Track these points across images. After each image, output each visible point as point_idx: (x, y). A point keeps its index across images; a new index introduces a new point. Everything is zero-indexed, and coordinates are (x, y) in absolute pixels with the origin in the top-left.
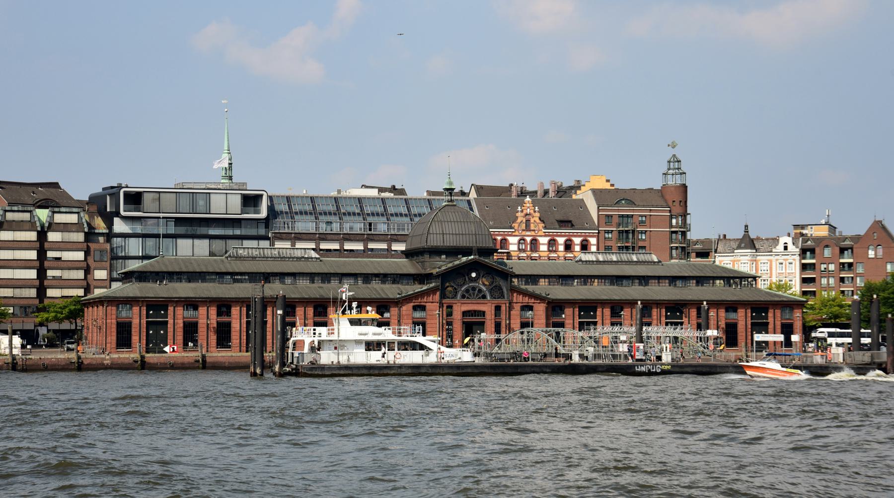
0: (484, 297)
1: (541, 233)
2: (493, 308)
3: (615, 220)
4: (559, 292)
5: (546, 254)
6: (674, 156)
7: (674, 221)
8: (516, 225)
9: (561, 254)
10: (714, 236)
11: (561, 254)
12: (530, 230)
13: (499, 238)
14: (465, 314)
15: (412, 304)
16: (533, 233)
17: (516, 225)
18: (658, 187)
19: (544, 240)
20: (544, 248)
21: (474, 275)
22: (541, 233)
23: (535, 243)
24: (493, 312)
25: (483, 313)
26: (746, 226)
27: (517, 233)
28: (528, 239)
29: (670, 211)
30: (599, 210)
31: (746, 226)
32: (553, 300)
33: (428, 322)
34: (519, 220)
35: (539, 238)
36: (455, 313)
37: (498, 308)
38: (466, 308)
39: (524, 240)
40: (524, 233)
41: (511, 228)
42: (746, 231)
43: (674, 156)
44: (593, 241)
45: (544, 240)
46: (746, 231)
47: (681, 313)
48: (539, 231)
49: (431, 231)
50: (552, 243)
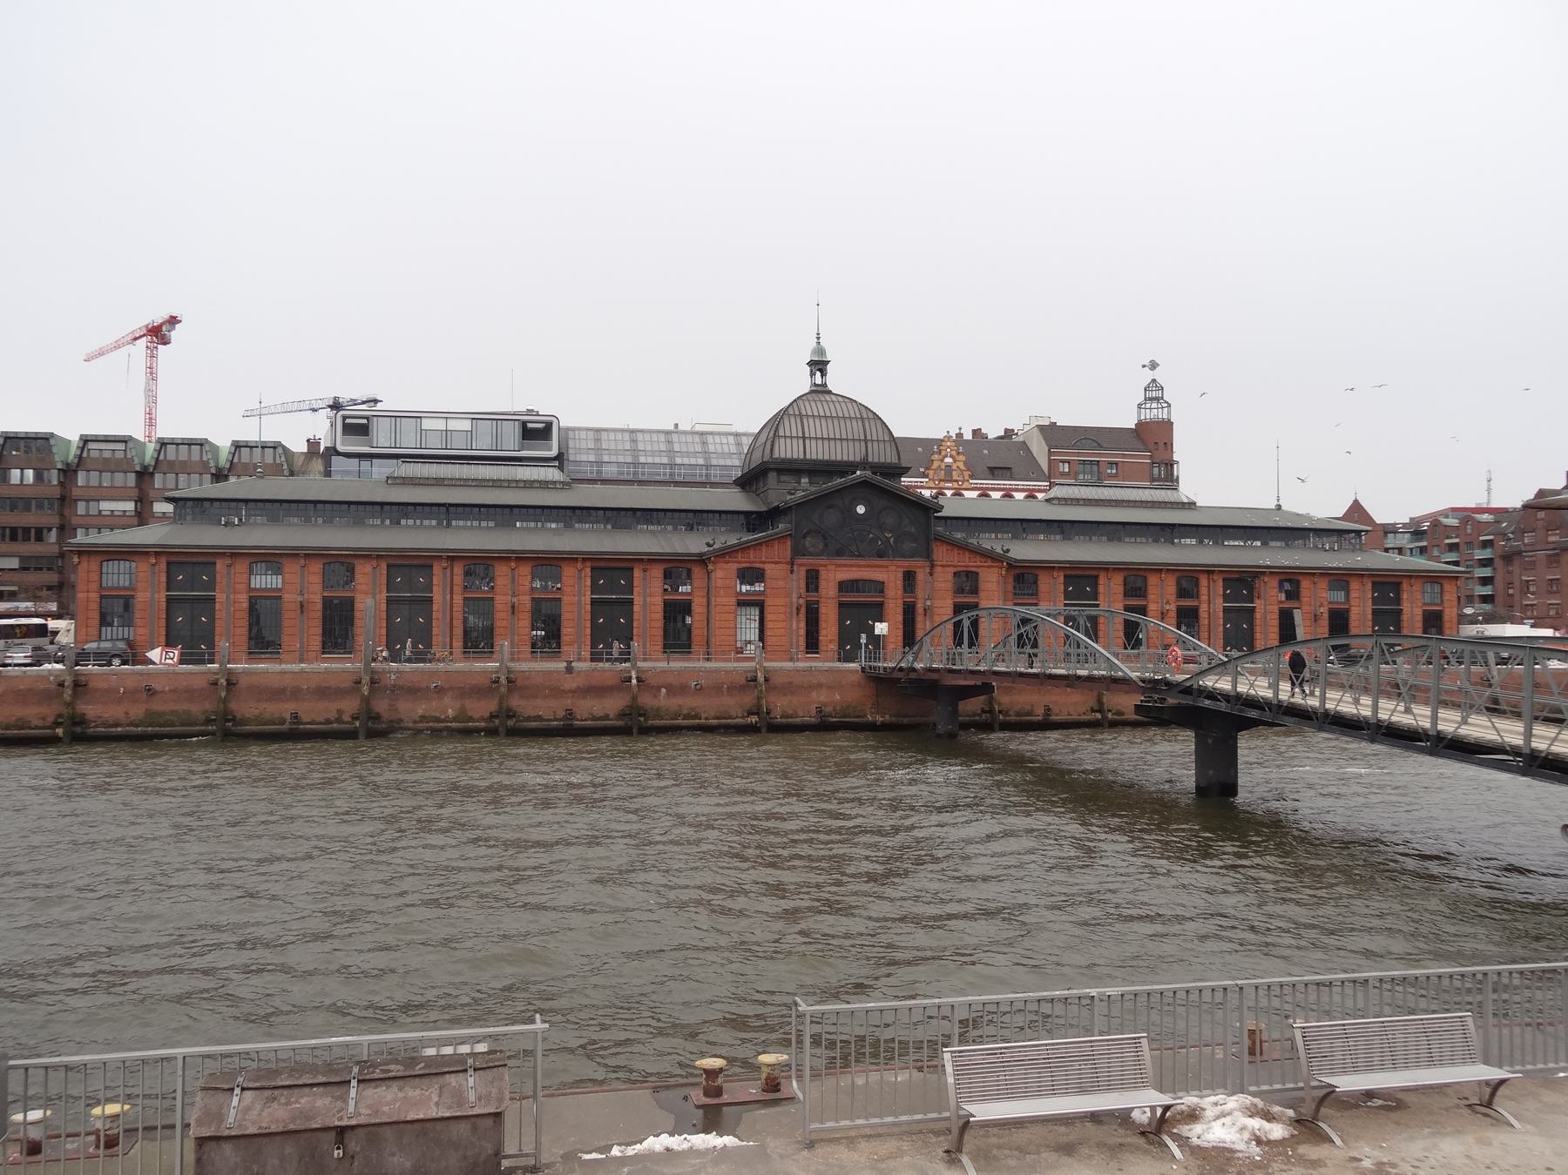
2: (900, 576)
4: (1025, 550)
6: (1154, 381)
7: (1156, 470)
8: (931, 473)
12: (951, 481)
14: (844, 586)
15: (736, 566)
17: (931, 473)
18: (1131, 423)
24: (900, 583)
25: (880, 587)
30: (1050, 454)
33: (768, 602)
34: (935, 465)
36: (823, 584)
37: (909, 578)
43: (1154, 381)
47: (1251, 590)
49: (781, 433)
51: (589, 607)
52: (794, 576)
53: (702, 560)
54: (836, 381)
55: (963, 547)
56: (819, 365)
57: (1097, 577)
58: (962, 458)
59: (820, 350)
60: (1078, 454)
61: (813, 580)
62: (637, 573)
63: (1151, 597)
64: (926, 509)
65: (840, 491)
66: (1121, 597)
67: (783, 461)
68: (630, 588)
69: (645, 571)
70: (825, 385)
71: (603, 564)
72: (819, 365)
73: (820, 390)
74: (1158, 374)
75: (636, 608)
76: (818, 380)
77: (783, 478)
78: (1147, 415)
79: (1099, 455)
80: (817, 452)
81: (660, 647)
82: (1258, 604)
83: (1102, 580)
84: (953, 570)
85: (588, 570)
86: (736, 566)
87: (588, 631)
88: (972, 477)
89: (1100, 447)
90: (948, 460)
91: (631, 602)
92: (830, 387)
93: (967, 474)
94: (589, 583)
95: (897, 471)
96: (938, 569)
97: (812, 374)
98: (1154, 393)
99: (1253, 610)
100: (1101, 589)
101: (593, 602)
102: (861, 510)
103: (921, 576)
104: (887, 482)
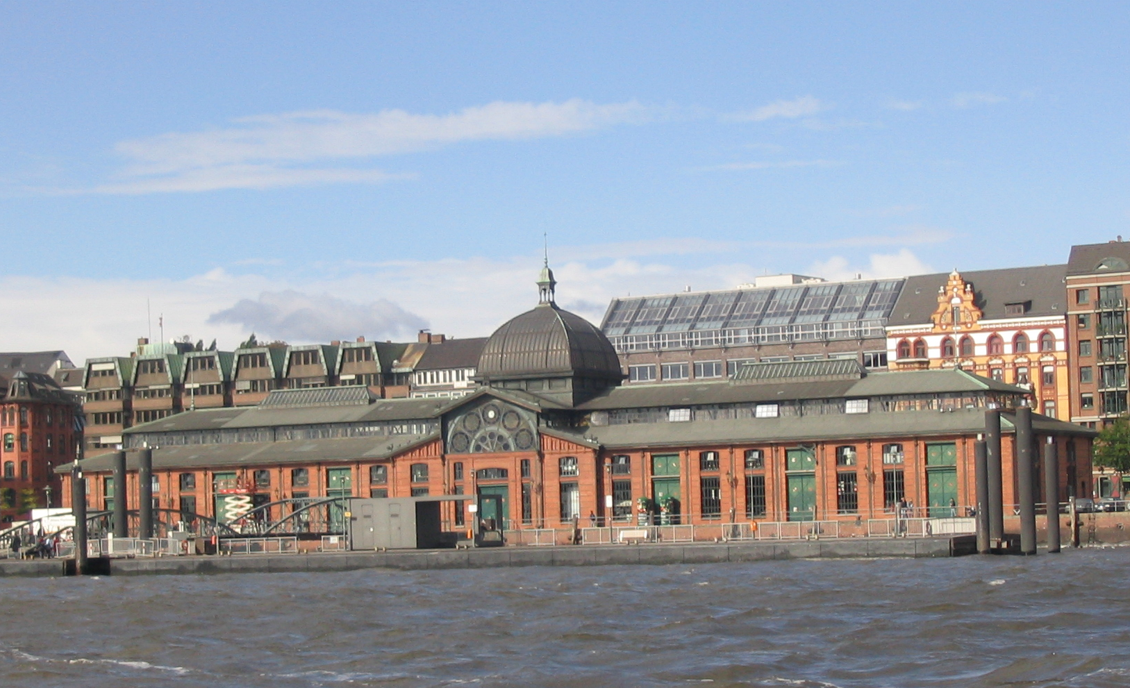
0: (506, 447)
2: (519, 464)
3: (1091, 297)
5: (984, 361)
8: (937, 317)
9: (1034, 358)
10: (134, 347)
11: (1034, 358)
13: (912, 340)
14: (478, 474)
16: (963, 328)
17: (937, 317)
19: (980, 339)
20: (980, 350)
23: (967, 345)
25: (503, 473)
27: (938, 329)
34: (941, 309)
35: (972, 335)
38: (480, 465)
41: (929, 322)
44: (1059, 333)
45: (980, 339)
50: (994, 343)
60: (1097, 280)
61: (458, 468)
88: (983, 317)
90: (956, 301)
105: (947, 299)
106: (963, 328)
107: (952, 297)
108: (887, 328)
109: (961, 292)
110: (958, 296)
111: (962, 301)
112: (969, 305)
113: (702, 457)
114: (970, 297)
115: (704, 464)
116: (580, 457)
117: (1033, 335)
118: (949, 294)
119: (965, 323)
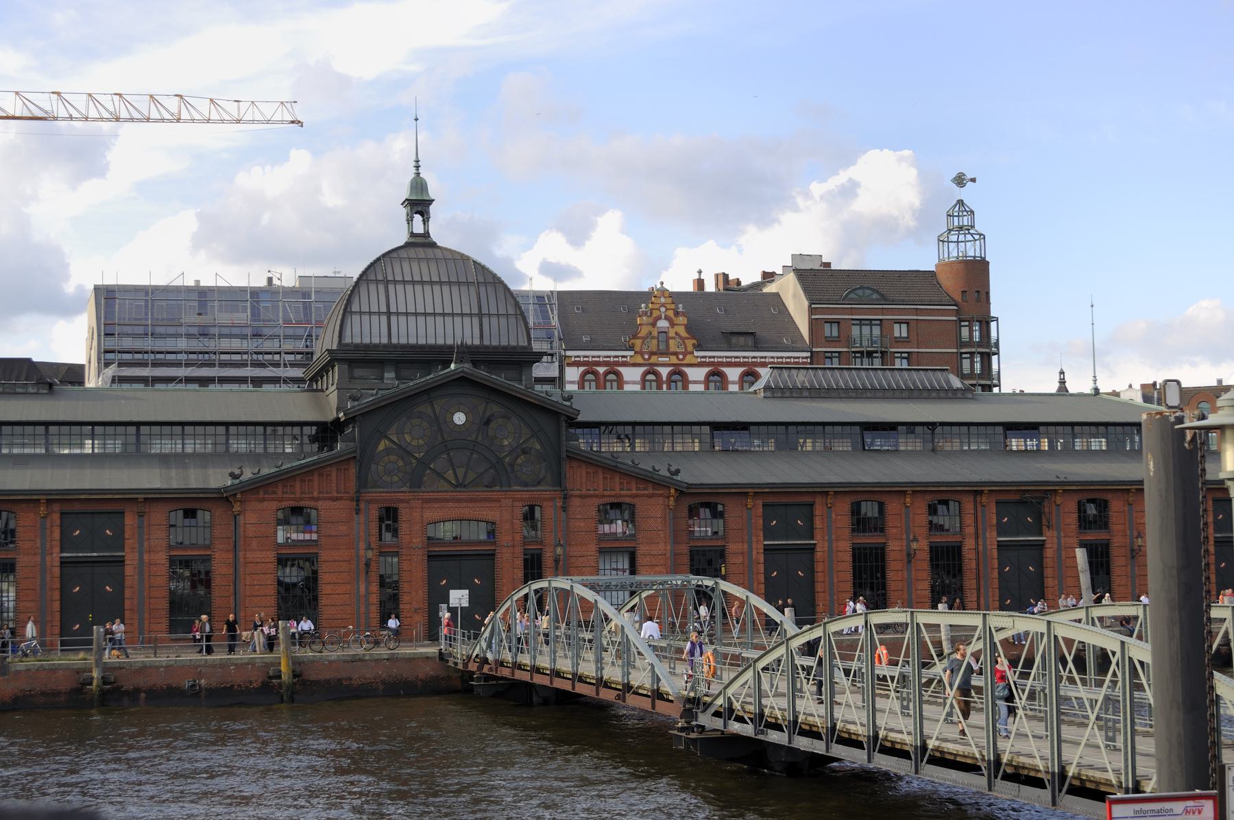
1: (689, 359)
7: (965, 332)
8: (638, 342)
12: (666, 353)
16: (674, 360)
17: (638, 342)
19: (697, 374)
21: (459, 418)
22: (689, 359)
26: (1062, 373)
27: (639, 360)
28: (664, 372)
29: (958, 312)
31: (1062, 373)
32: (690, 486)
34: (644, 332)
39: (656, 373)
40: (654, 359)
42: (1062, 382)
46: (1062, 382)
47: (1038, 517)
48: (685, 354)
51: (57, 571)
52: (362, 518)
53: (223, 498)
54: (444, 230)
55: (610, 467)
56: (419, 205)
57: (811, 505)
58: (682, 320)
59: (419, 184)
60: (852, 311)
62: (130, 520)
63: (891, 531)
64: (559, 418)
65: (427, 393)
66: (847, 532)
67: (357, 347)
68: (118, 541)
69: (141, 515)
70: (426, 235)
71: (77, 507)
72: (419, 205)
73: (421, 242)
74: (967, 194)
75: (128, 570)
76: (418, 227)
77: (358, 372)
78: (954, 252)
79: (883, 311)
80: (410, 333)
81: (165, 624)
82: (1048, 537)
83: (818, 510)
84: (597, 501)
85: (56, 517)
86: (275, 505)
87: (57, 605)
88: (699, 347)
89: (884, 299)
90: (663, 324)
91: (121, 562)
92: (435, 236)
93: (690, 343)
94: (57, 535)
95: (522, 359)
96: (576, 502)
97: (410, 220)
98: (961, 220)
99: (1041, 546)
100: (818, 523)
101: (64, 563)
102: (459, 418)
103: (548, 513)
104: (499, 379)
105: (651, 320)
106: (674, 360)
107: (659, 318)
108: (569, 353)
109: (671, 313)
110: (667, 318)
111: (672, 324)
112: (682, 331)
113: (856, 510)
114: (682, 320)
115: (860, 524)
116: (642, 507)
117: (733, 374)
118: (655, 314)
119: (676, 354)
